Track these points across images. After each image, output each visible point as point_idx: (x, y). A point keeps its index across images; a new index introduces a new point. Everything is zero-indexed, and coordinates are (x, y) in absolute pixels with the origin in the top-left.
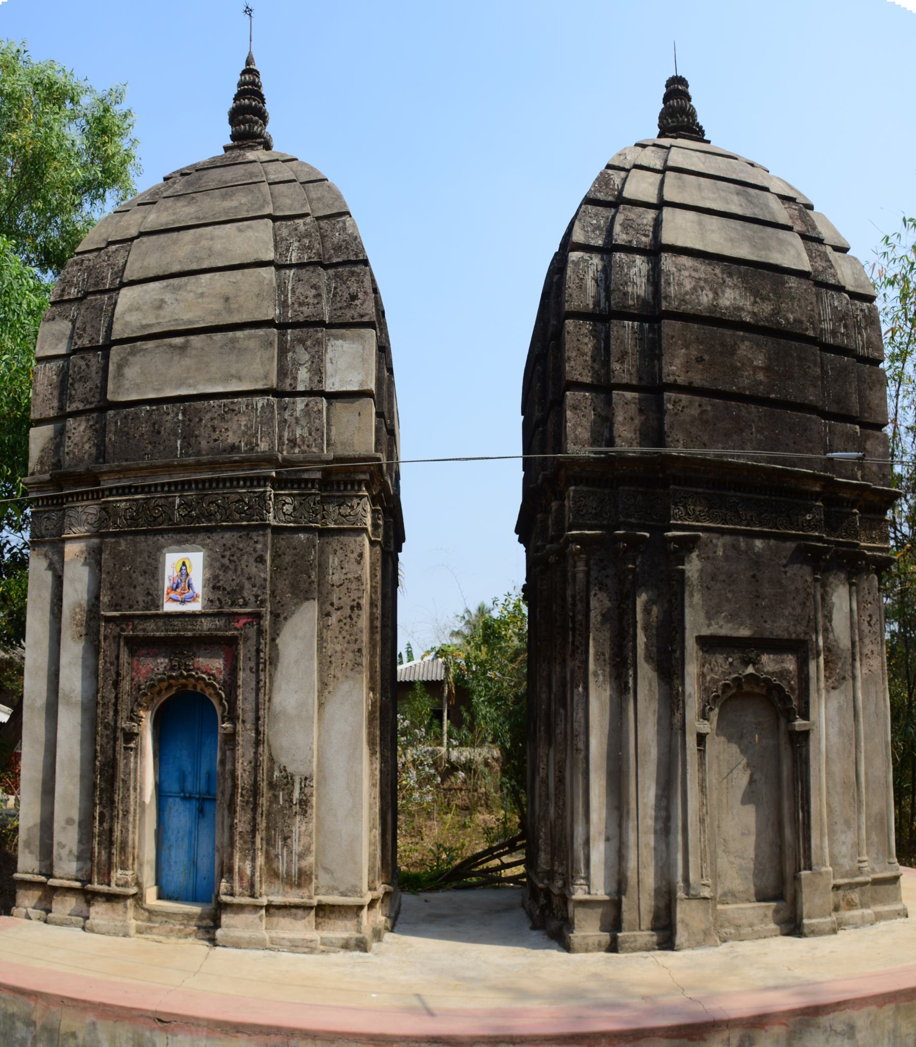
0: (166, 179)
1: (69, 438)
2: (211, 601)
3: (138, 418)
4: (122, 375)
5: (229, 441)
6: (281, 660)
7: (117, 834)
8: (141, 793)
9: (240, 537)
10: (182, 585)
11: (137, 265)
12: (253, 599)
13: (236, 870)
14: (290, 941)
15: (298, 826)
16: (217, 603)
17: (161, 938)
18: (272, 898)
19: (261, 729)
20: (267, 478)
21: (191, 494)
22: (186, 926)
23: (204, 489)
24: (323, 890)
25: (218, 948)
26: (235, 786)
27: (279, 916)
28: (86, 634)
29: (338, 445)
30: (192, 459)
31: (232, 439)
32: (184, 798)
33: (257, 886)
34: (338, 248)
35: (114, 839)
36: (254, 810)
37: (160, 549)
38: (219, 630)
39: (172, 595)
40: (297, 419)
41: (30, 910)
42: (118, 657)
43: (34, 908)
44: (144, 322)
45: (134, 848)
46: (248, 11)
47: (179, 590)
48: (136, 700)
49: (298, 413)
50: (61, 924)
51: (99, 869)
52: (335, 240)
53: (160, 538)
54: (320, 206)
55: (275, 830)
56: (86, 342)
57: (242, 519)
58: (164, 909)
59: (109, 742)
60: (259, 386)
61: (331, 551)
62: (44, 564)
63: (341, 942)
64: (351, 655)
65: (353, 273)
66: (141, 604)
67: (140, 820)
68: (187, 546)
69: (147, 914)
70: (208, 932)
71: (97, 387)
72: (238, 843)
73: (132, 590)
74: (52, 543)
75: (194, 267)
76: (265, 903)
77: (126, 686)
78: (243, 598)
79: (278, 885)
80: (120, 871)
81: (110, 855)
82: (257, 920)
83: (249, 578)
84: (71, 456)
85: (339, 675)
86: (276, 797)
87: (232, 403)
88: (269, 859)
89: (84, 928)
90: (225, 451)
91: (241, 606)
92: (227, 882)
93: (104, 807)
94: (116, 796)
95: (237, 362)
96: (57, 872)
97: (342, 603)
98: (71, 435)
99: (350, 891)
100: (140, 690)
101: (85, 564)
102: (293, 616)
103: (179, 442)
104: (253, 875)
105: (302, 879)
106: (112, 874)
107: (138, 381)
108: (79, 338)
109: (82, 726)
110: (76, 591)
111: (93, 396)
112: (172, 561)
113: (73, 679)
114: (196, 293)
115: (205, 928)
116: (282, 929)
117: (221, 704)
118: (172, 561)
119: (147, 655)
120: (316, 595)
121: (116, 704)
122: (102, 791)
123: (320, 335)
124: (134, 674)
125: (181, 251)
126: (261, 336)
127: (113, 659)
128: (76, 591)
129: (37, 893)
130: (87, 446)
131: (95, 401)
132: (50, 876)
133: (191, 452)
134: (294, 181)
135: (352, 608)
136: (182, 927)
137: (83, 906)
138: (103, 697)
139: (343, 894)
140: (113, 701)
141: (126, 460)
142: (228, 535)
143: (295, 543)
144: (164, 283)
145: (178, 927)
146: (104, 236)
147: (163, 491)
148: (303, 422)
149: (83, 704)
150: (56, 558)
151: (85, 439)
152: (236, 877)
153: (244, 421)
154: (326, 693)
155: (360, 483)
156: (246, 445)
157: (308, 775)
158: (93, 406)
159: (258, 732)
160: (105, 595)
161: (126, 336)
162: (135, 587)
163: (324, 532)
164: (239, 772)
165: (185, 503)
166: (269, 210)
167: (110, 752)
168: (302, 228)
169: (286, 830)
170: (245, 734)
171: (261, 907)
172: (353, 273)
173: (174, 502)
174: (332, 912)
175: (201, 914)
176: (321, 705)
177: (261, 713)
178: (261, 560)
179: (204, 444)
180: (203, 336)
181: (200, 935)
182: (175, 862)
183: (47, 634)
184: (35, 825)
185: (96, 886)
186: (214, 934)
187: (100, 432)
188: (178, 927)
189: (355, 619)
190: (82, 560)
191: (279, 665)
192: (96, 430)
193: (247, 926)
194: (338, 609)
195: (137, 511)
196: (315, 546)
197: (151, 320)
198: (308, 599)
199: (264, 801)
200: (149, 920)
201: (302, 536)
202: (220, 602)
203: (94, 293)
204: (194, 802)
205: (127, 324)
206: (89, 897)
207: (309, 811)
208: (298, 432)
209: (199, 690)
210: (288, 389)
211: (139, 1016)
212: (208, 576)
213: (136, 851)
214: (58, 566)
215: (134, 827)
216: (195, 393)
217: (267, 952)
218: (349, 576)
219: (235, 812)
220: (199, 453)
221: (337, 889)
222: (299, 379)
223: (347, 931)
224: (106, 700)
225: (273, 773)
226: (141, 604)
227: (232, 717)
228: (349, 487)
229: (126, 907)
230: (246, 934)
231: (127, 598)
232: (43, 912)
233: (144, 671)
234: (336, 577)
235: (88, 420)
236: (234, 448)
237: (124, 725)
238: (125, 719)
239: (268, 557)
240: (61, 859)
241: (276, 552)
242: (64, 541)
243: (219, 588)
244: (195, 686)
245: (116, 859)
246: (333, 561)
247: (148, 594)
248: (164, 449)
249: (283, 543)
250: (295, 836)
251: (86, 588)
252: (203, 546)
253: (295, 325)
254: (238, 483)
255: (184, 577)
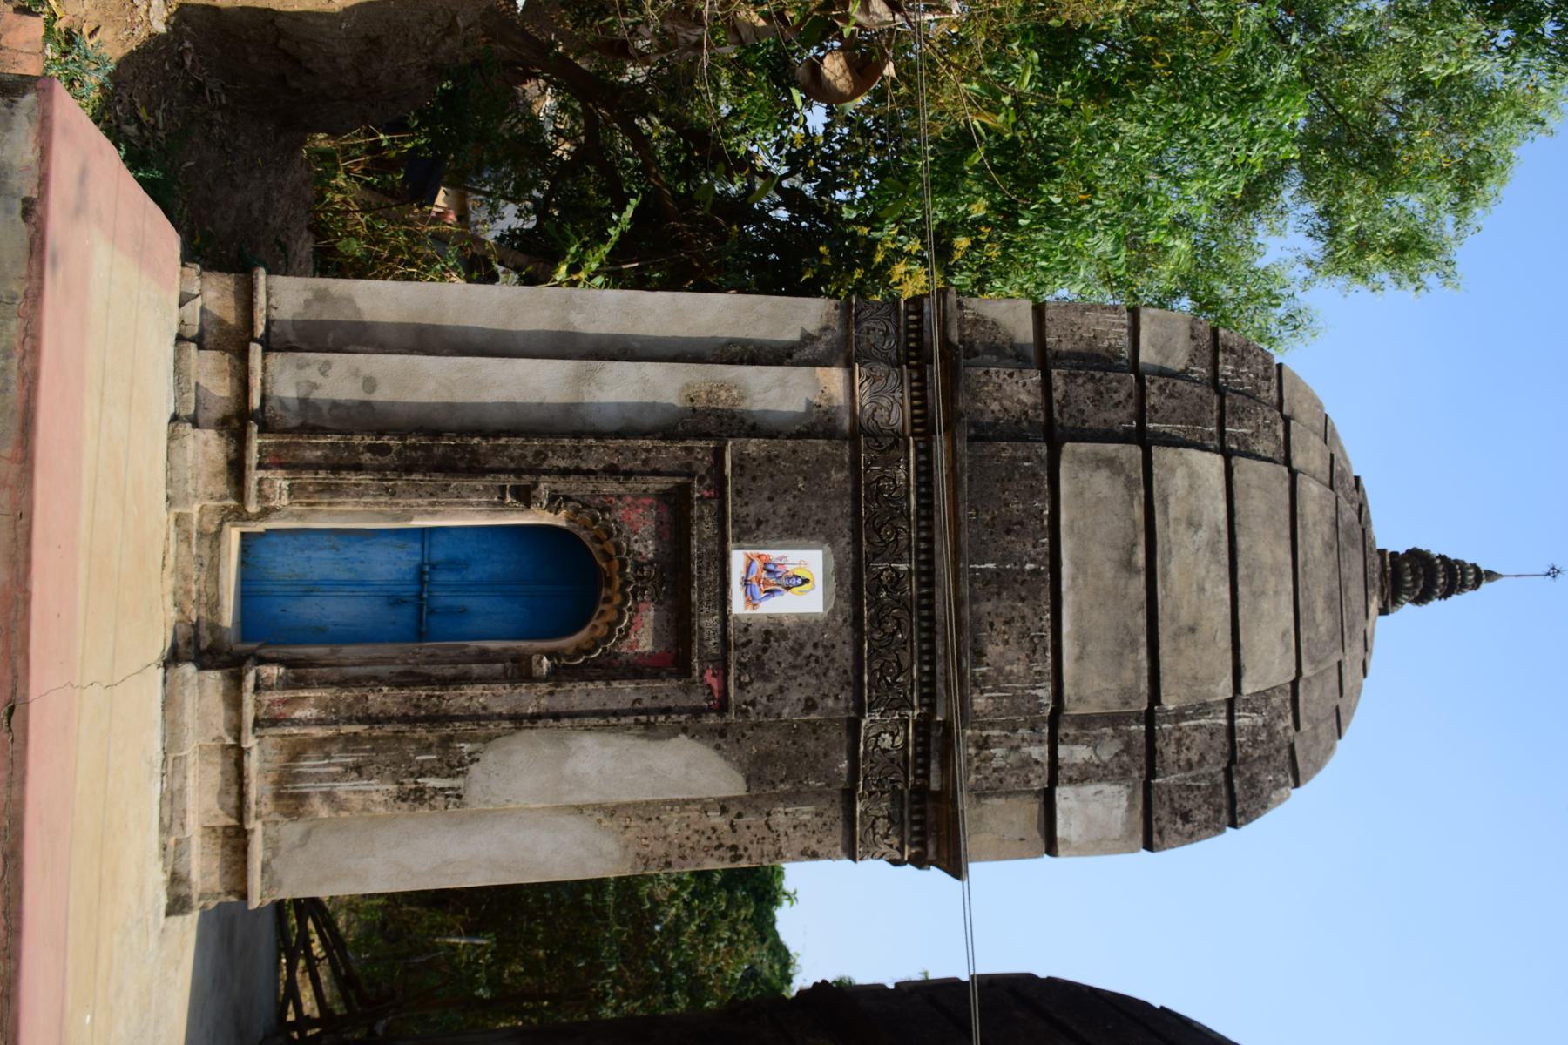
0: (1357, 479)
1: (1011, 375)
2: (746, 630)
3: (1033, 496)
4: (1098, 467)
5: (990, 648)
6: (653, 744)
7: (353, 478)
8: (427, 512)
9: (845, 672)
10: (773, 581)
11: (1253, 478)
12: (749, 697)
13: (301, 694)
14: (182, 789)
15: (380, 789)
16: (744, 640)
17: (171, 561)
18: (255, 753)
19: (540, 724)
20: (932, 707)
21: (912, 588)
22: (197, 602)
23: (920, 607)
24: (271, 832)
25: (161, 670)
26: (445, 682)
27: (223, 764)
28: (694, 410)
29: (978, 810)
30: (966, 591)
31: (993, 651)
32: (420, 572)
33: (275, 731)
34: (1252, 783)
35: (344, 474)
36: (405, 719)
37: (830, 539)
38: (700, 644)
39: (757, 564)
40: (1018, 748)
41: (198, 302)
42: (656, 473)
43: (203, 310)
44: (1172, 500)
45: (330, 504)
46: (1554, 572)
47: (764, 574)
48: (585, 506)
49: (1025, 749)
50: (179, 372)
51: (287, 446)
52: (1261, 778)
53: (847, 539)
54: (1308, 743)
55: (372, 750)
56: (1152, 400)
57: (871, 674)
58: (223, 562)
59: (512, 459)
60: (1068, 690)
61: (821, 809)
62: (812, 327)
63: (183, 871)
64: (661, 852)
65: (1218, 811)
66: (743, 511)
67: (380, 513)
68: (833, 585)
69: (213, 529)
70: (188, 643)
71: (1084, 422)
72: (347, 695)
73: (766, 494)
74: (845, 340)
75: (1241, 571)
76: (248, 827)
77: (609, 487)
78: (751, 682)
79: (277, 760)
80: (285, 484)
81: (314, 467)
82: (215, 733)
83: (781, 690)
84: (983, 379)
85: (630, 834)
86: (427, 749)
87: (1045, 649)
88: (321, 743)
89: (175, 418)
90: (976, 641)
91: (738, 678)
92: (280, 678)
93: (399, 453)
94: (420, 477)
95: (1103, 653)
96: (275, 359)
97: (742, 830)
98: (1015, 378)
99: (271, 877)
100: (603, 511)
101: (810, 405)
102: (722, 761)
103: (992, 566)
104: (295, 722)
105: (290, 801)
106: (280, 473)
107: (1087, 495)
108: (1160, 388)
109: (540, 405)
110: (767, 390)
111: (1071, 416)
112: (810, 561)
113: (623, 387)
114: (1204, 579)
115: (197, 636)
116: (202, 772)
117: (579, 651)
118: (810, 561)
119: (660, 522)
120: (755, 792)
121: (577, 471)
122: (427, 448)
123: (1136, 774)
124: (629, 499)
125: (1264, 548)
126: (1138, 687)
127: (653, 465)
128: (767, 390)
129: (232, 317)
130: (995, 406)
131: (1063, 420)
132: (268, 348)
133: (977, 586)
134: (1341, 694)
135: (734, 848)
136: (194, 596)
137: (215, 413)
138: (590, 447)
139: (266, 866)
140: (584, 466)
141: (970, 479)
142: (848, 651)
143: (834, 755)
144: (1224, 527)
145: (194, 588)
146: (1298, 410)
147: (919, 539)
148: (1013, 759)
149: (577, 405)
150: (821, 347)
151: (1007, 403)
152: (288, 694)
153: (1018, 669)
154: (599, 816)
155: (923, 844)
156: (983, 675)
157: (466, 799)
158: (1056, 416)
159: (535, 718)
160: (758, 446)
161: (1155, 470)
162: (771, 499)
163: (849, 796)
164: (468, 691)
165: (899, 579)
166: (1307, 671)
167: (495, 463)
168: (1281, 725)
169: (373, 769)
170: (530, 699)
171: (238, 738)
172: (1218, 811)
173: (901, 561)
174: (234, 849)
175: (220, 628)
176: (579, 809)
177: (566, 722)
178: (810, 705)
179: (987, 606)
180: (1143, 595)
181: (183, 629)
182: (309, 559)
183: (694, 334)
184: (358, 311)
185: (255, 442)
186: (188, 660)
187: (1014, 431)
188: (194, 588)
189: (717, 853)
190: (816, 400)
191: (645, 741)
192: (1019, 422)
193: (203, 716)
194: (732, 825)
195: (890, 499)
196: (829, 785)
197: (1175, 510)
198: (748, 781)
199: (421, 731)
200: (202, 534)
201: (845, 765)
202: (745, 645)
203: (1222, 407)
204: (416, 588)
205: (1172, 471)
206: (236, 423)
207: (405, 806)
208: (998, 752)
209: (602, 607)
210: (1061, 732)
211: (14, 671)
212: (786, 622)
213: (325, 508)
214: (807, 352)
215: (366, 504)
216: (1064, 589)
217: (161, 756)
218: (783, 839)
219: (401, 686)
220: (975, 599)
221: (275, 855)
222: (1075, 748)
223: (203, 876)
224: (584, 453)
225: (467, 741)
226: (743, 511)
227: (563, 673)
228: (916, 828)
229: (222, 497)
230: (189, 717)
231: (753, 486)
232: (196, 330)
233: (633, 516)
234: (781, 818)
235: (1035, 408)
236: (979, 654)
237: (542, 486)
238: (553, 487)
239: (813, 717)
240: (300, 367)
241: (821, 726)
242: (849, 366)
243: (767, 641)
244: (608, 600)
245: (307, 477)
246: (805, 813)
247: (759, 523)
248: (983, 542)
249: (834, 736)
250: (362, 784)
251: (770, 408)
252: (833, 613)
253: (1151, 736)
254: (927, 663)
255: (784, 582)
